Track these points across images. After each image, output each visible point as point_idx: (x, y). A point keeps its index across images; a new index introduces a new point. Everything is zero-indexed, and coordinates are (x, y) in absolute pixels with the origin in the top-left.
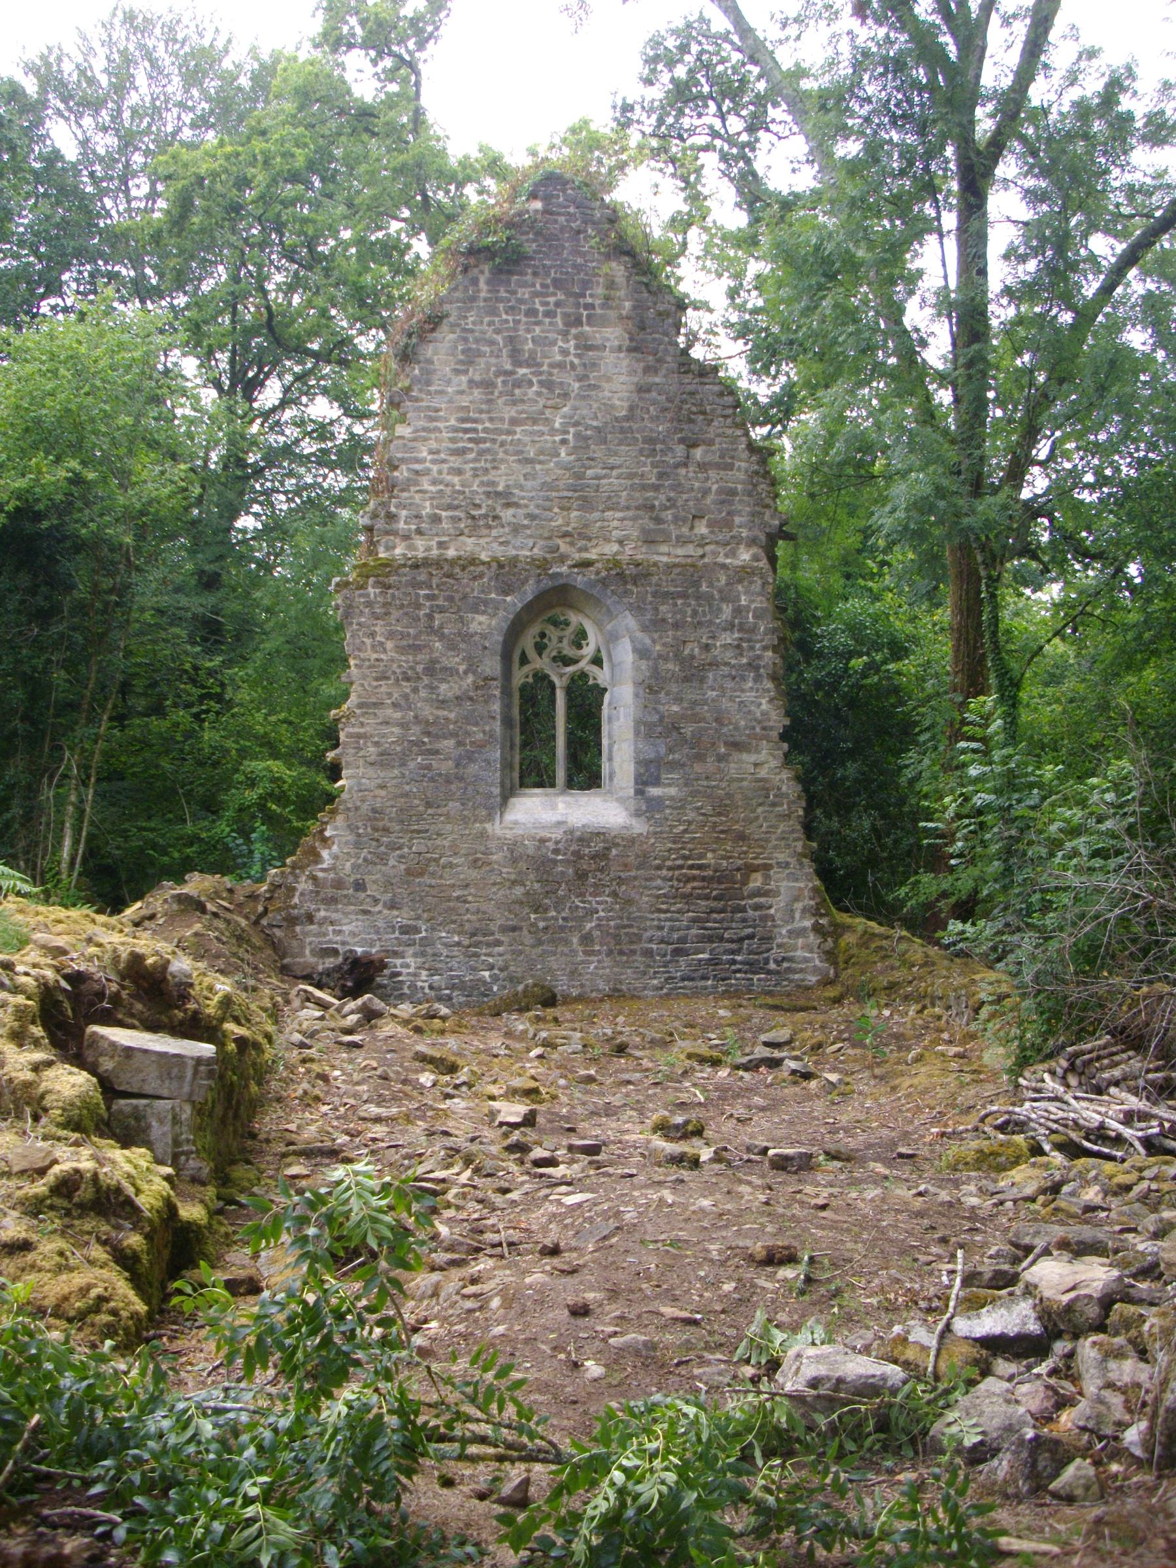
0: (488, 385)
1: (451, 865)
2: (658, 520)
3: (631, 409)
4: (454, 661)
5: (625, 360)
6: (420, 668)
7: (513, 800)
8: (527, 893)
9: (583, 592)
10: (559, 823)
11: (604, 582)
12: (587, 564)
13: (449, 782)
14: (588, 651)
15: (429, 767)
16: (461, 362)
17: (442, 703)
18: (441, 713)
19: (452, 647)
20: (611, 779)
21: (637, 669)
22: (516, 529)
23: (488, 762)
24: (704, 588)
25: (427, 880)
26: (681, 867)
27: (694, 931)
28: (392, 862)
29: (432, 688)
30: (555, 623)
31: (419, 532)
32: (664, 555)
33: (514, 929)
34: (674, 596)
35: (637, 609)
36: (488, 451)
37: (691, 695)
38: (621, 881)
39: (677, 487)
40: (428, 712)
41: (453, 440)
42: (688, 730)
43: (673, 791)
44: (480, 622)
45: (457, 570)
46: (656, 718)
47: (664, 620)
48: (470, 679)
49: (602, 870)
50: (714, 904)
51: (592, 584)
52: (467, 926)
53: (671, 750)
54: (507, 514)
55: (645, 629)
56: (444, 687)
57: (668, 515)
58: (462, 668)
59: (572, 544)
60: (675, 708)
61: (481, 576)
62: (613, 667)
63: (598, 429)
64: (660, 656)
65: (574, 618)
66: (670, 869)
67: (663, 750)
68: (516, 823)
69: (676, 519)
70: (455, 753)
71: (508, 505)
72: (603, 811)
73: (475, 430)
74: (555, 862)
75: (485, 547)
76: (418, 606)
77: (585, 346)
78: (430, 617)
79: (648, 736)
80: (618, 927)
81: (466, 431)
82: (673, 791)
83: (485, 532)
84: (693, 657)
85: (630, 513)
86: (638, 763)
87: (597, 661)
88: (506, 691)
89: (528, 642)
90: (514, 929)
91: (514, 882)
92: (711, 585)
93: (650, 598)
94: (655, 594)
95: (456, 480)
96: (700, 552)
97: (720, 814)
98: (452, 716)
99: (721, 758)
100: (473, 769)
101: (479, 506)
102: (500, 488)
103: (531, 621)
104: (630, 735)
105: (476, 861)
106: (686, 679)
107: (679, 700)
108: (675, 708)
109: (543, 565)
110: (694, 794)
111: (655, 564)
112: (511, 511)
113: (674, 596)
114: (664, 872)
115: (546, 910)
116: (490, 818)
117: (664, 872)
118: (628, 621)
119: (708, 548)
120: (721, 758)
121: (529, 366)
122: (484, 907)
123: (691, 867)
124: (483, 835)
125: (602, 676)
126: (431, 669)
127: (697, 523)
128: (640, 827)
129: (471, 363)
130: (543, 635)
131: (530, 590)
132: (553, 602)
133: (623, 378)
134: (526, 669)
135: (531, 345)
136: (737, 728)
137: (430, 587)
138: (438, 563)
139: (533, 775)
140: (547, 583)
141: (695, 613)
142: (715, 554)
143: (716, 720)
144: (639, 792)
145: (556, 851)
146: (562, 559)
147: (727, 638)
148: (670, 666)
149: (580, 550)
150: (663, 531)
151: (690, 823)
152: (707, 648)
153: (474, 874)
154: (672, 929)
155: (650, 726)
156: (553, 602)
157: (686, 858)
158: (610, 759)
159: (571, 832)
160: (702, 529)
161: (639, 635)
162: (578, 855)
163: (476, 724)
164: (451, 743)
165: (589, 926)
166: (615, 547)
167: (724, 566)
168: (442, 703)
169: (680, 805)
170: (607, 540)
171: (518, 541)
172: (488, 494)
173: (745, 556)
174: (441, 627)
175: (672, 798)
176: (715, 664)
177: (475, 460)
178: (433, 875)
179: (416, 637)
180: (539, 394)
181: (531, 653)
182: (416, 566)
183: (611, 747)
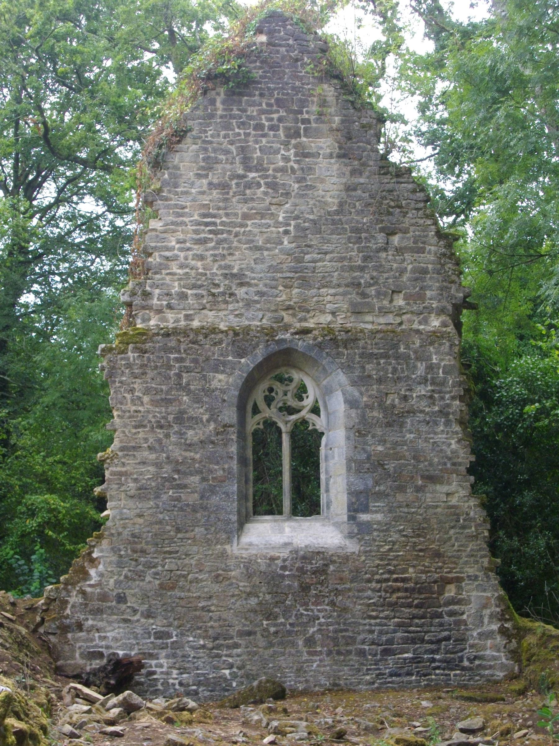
0: (224, 187)
1: (197, 581)
2: (364, 295)
3: (341, 204)
4: (201, 412)
5: (335, 166)
6: (171, 418)
7: (248, 526)
8: (260, 603)
9: (304, 354)
10: (286, 544)
11: (320, 346)
12: (306, 331)
13: (195, 511)
14: (308, 402)
15: (178, 499)
16: (203, 168)
17: (189, 446)
18: (188, 454)
19: (197, 400)
20: (328, 507)
21: (348, 416)
22: (249, 304)
23: (227, 494)
24: (402, 350)
25: (177, 593)
26: (387, 580)
27: (399, 635)
28: (148, 578)
29: (181, 434)
30: (280, 379)
31: (170, 307)
32: (369, 323)
33: (249, 633)
34: (378, 357)
35: (348, 368)
36: (225, 240)
37: (393, 437)
38: (338, 592)
39: (379, 268)
40: (178, 454)
41: (196, 232)
42: (391, 466)
43: (379, 517)
44: (220, 380)
45: (201, 337)
46: (364, 456)
47: (369, 376)
48: (212, 426)
49: (321, 583)
50: (415, 611)
51: (311, 348)
52: (211, 632)
53: (377, 483)
54: (241, 292)
55: (354, 383)
56: (190, 433)
57: (372, 291)
58: (205, 417)
59: (294, 315)
60: (380, 448)
61: (220, 342)
62: (328, 415)
63: (314, 222)
64: (367, 406)
65: (296, 376)
66: (378, 581)
67: (370, 483)
68: (251, 544)
69: (378, 294)
70: (200, 487)
71: (241, 284)
72: (322, 534)
73: (214, 224)
74: (283, 577)
75: (224, 319)
76: (170, 367)
77: (303, 154)
78: (179, 376)
80: (336, 631)
81: (207, 224)
82: (379, 517)
83: (223, 306)
84: (393, 406)
85: (341, 290)
86: (350, 493)
87: (315, 410)
88: (242, 436)
89: (259, 395)
90: (249, 633)
91: (249, 594)
92: (407, 347)
93: (357, 359)
94: (362, 355)
95: (199, 264)
96: (398, 320)
97: (419, 536)
98: (198, 456)
99: (419, 489)
100: (215, 500)
101: (218, 286)
102: (235, 271)
103: (262, 379)
104: (343, 470)
105: (218, 576)
106: (389, 425)
107: (383, 442)
108: (380, 448)
109: (269, 333)
110: (396, 519)
111: (362, 331)
112: (244, 289)
113: (378, 357)
114: (374, 585)
115: (276, 618)
116: (229, 540)
117: (374, 585)
118: (341, 378)
119: (405, 317)
120: (419, 489)
121: (257, 171)
122: (225, 615)
123: (396, 580)
124: (223, 555)
125: (320, 423)
126: (180, 418)
127: (395, 296)
128: (352, 547)
129: (210, 169)
130: (271, 390)
131: (260, 354)
132: (278, 362)
133: (334, 180)
134: (258, 417)
135: (259, 154)
136: (431, 464)
137: (179, 352)
138: (185, 332)
139: (264, 504)
140: (274, 348)
141: (395, 370)
142: (411, 322)
143: (414, 458)
144: (352, 518)
145: (284, 568)
146: (286, 328)
147: (422, 390)
148: (375, 414)
149: (301, 320)
150: (368, 304)
151: (394, 543)
152: (405, 398)
153: (216, 587)
154: (381, 633)
155: (360, 463)
156: (278, 362)
157: (390, 572)
158: (327, 491)
159: (296, 552)
160: (400, 301)
161: (349, 388)
162: (301, 570)
163: (218, 463)
164: (196, 479)
165: (312, 630)
166: (329, 318)
167: (418, 331)
168: (189, 446)
169: (386, 528)
170: (323, 312)
171: (250, 314)
172: (225, 276)
173: (435, 323)
174: (188, 384)
175: (379, 523)
176: (412, 412)
177: (214, 248)
178: (182, 589)
179: (167, 393)
180: (266, 194)
181: (262, 405)
182: (167, 335)
183: (327, 480)
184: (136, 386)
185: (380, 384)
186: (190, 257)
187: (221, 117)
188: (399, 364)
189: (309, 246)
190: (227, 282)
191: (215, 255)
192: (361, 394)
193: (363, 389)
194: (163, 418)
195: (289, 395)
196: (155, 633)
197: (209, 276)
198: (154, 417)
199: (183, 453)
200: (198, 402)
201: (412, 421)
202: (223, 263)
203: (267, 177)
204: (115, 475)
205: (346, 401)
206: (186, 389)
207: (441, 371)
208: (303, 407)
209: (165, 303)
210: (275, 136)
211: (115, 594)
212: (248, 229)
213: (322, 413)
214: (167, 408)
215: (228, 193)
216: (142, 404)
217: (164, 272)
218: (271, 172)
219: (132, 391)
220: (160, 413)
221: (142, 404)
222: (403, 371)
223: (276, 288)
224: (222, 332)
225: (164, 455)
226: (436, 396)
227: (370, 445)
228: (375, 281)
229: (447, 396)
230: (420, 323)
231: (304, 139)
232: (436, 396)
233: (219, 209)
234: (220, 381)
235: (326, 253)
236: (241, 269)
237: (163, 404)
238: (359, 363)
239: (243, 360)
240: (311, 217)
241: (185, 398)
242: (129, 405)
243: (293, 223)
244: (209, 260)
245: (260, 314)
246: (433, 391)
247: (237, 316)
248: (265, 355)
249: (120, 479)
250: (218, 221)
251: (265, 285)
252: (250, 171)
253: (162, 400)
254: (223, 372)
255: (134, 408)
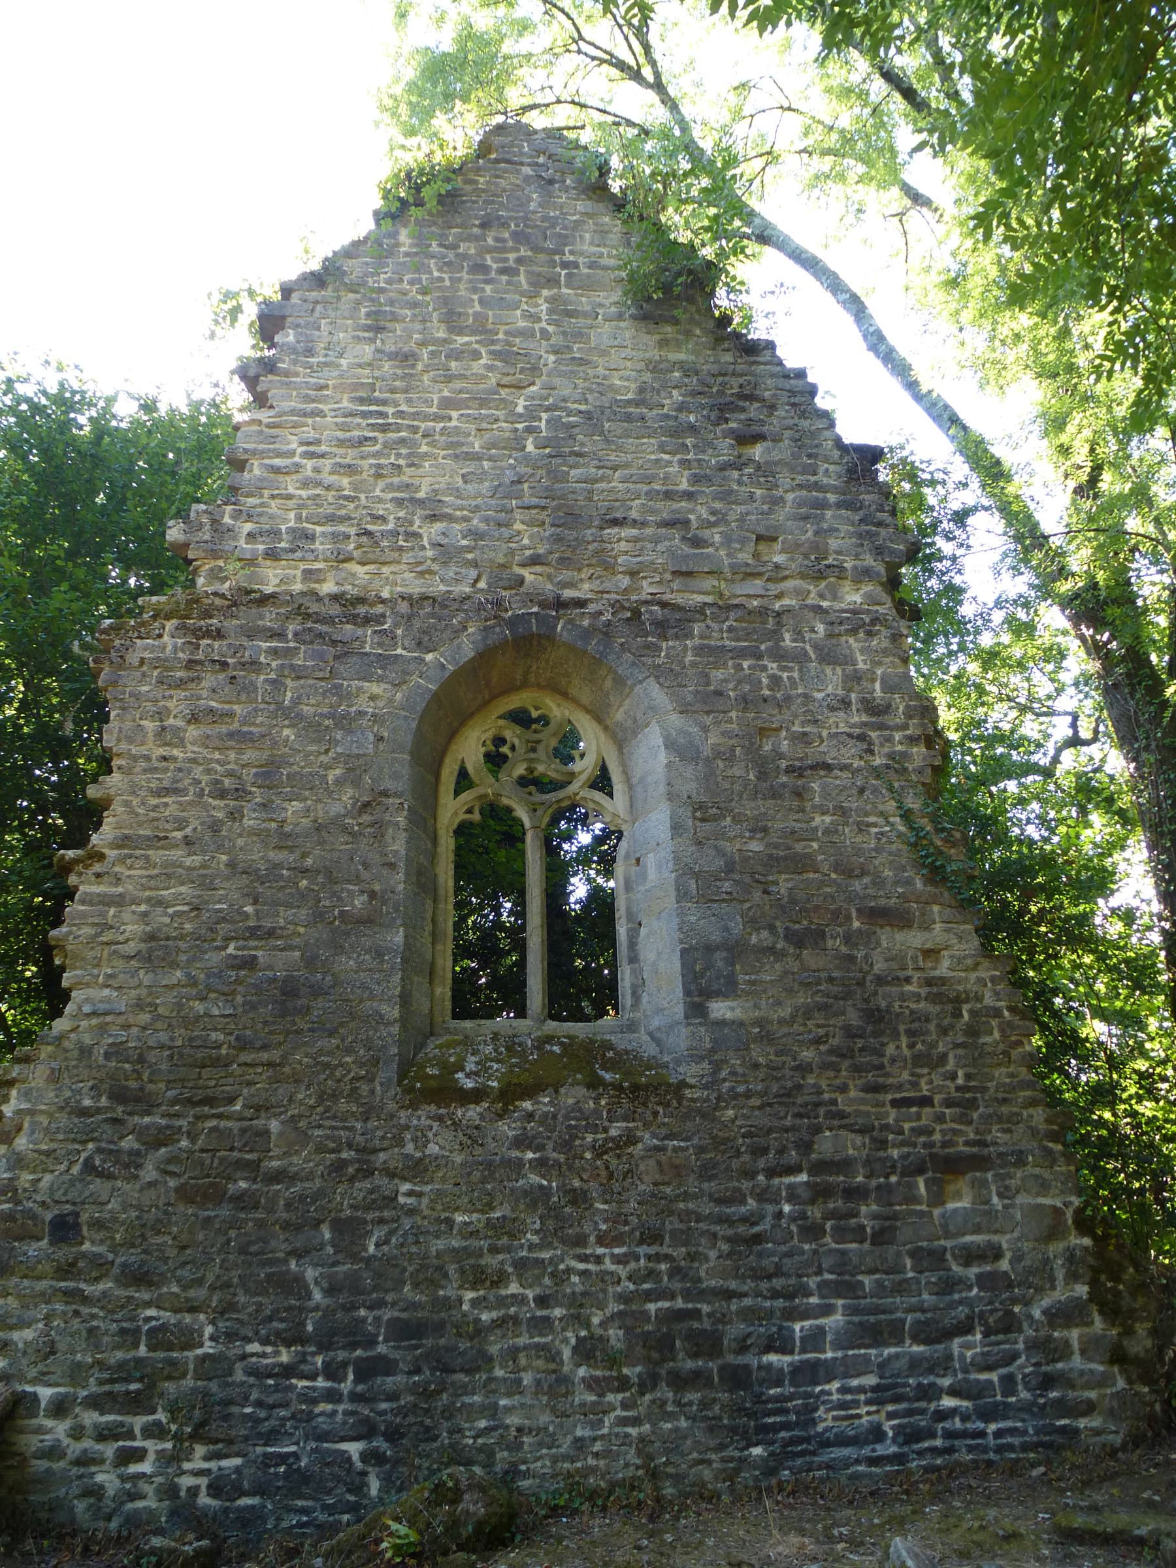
0: (406, 358)
3: (641, 390)
5: (628, 331)
6: (248, 775)
14: (584, 767)
16: (368, 328)
20: (636, 997)
23: (379, 953)
24: (787, 640)
28: (149, 1173)
35: (668, 675)
36: (402, 441)
39: (726, 496)
41: (344, 428)
44: (373, 695)
54: (431, 532)
60: (755, 846)
63: (588, 416)
69: (728, 540)
71: (433, 518)
73: (383, 415)
74: (517, 1166)
77: (562, 311)
78: (277, 684)
79: (706, 899)
81: (365, 415)
92: (799, 636)
93: (689, 658)
94: (699, 650)
95: (345, 481)
101: (383, 519)
102: (421, 495)
104: (670, 901)
107: (760, 829)
108: (755, 846)
121: (473, 333)
129: (379, 329)
133: (627, 352)
134: (466, 796)
135: (478, 308)
136: (879, 882)
141: (775, 681)
147: (840, 722)
148: (737, 771)
158: (633, 959)
166: (625, 581)
172: (399, 502)
173: (853, 596)
174: (296, 701)
177: (376, 455)
180: (490, 368)
184: (170, 704)
185: (745, 710)
186: (328, 469)
187: (407, 254)
188: (783, 669)
189: (579, 455)
190: (401, 514)
191: (379, 466)
192: (705, 729)
193: (708, 720)
194: (230, 774)
195: (541, 748)
196: (151, 1331)
197: (363, 501)
198: (208, 771)
199: (271, 854)
200: (318, 741)
201: (823, 787)
202: (396, 480)
203: (493, 342)
204: (91, 904)
205: (670, 745)
206: (290, 715)
207: (877, 686)
208: (572, 775)
209: (261, 547)
210: (509, 283)
211: (49, 1216)
212: (454, 423)
213: (618, 787)
214: (240, 752)
215: (413, 366)
216: (181, 743)
217: (266, 492)
218: (501, 336)
219: (161, 715)
220: (222, 763)
221: (181, 743)
222: (793, 683)
223: (507, 525)
224: (383, 601)
225: (224, 858)
226: (874, 735)
227: (730, 840)
228: (720, 519)
229: (897, 736)
230: (822, 596)
231: (565, 290)
232: (874, 735)
233: (392, 391)
234: (373, 698)
235: (615, 469)
236: (435, 491)
237: (232, 743)
238: (694, 664)
239: (429, 657)
240: (583, 408)
241: (286, 732)
242: (150, 745)
243: (544, 416)
244: (365, 475)
245: (473, 573)
246: (865, 724)
247: (422, 574)
248: (481, 647)
249: (102, 915)
250: (390, 410)
251: (486, 520)
252: (460, 334)
253: (231, 735)
254: (380, 680)
255: (161, 751)
